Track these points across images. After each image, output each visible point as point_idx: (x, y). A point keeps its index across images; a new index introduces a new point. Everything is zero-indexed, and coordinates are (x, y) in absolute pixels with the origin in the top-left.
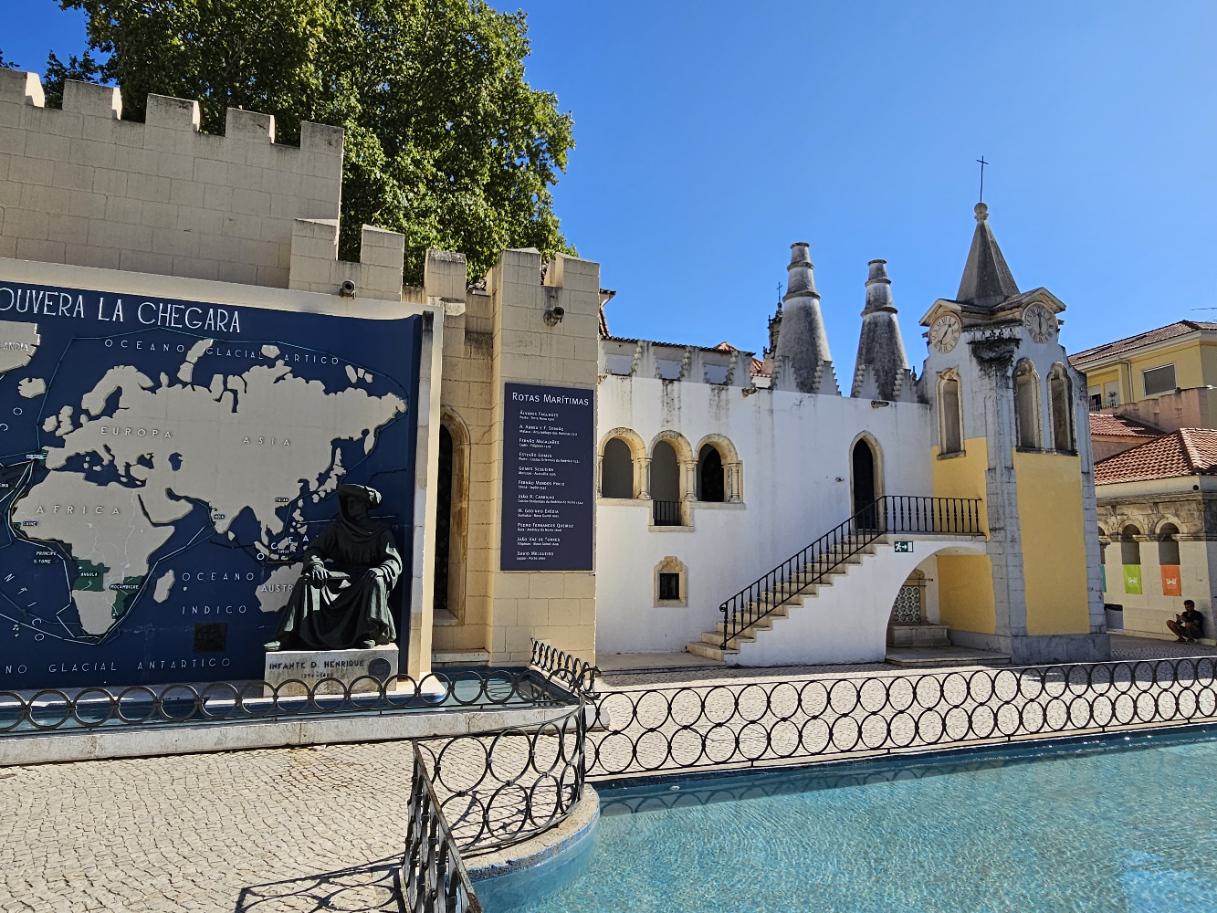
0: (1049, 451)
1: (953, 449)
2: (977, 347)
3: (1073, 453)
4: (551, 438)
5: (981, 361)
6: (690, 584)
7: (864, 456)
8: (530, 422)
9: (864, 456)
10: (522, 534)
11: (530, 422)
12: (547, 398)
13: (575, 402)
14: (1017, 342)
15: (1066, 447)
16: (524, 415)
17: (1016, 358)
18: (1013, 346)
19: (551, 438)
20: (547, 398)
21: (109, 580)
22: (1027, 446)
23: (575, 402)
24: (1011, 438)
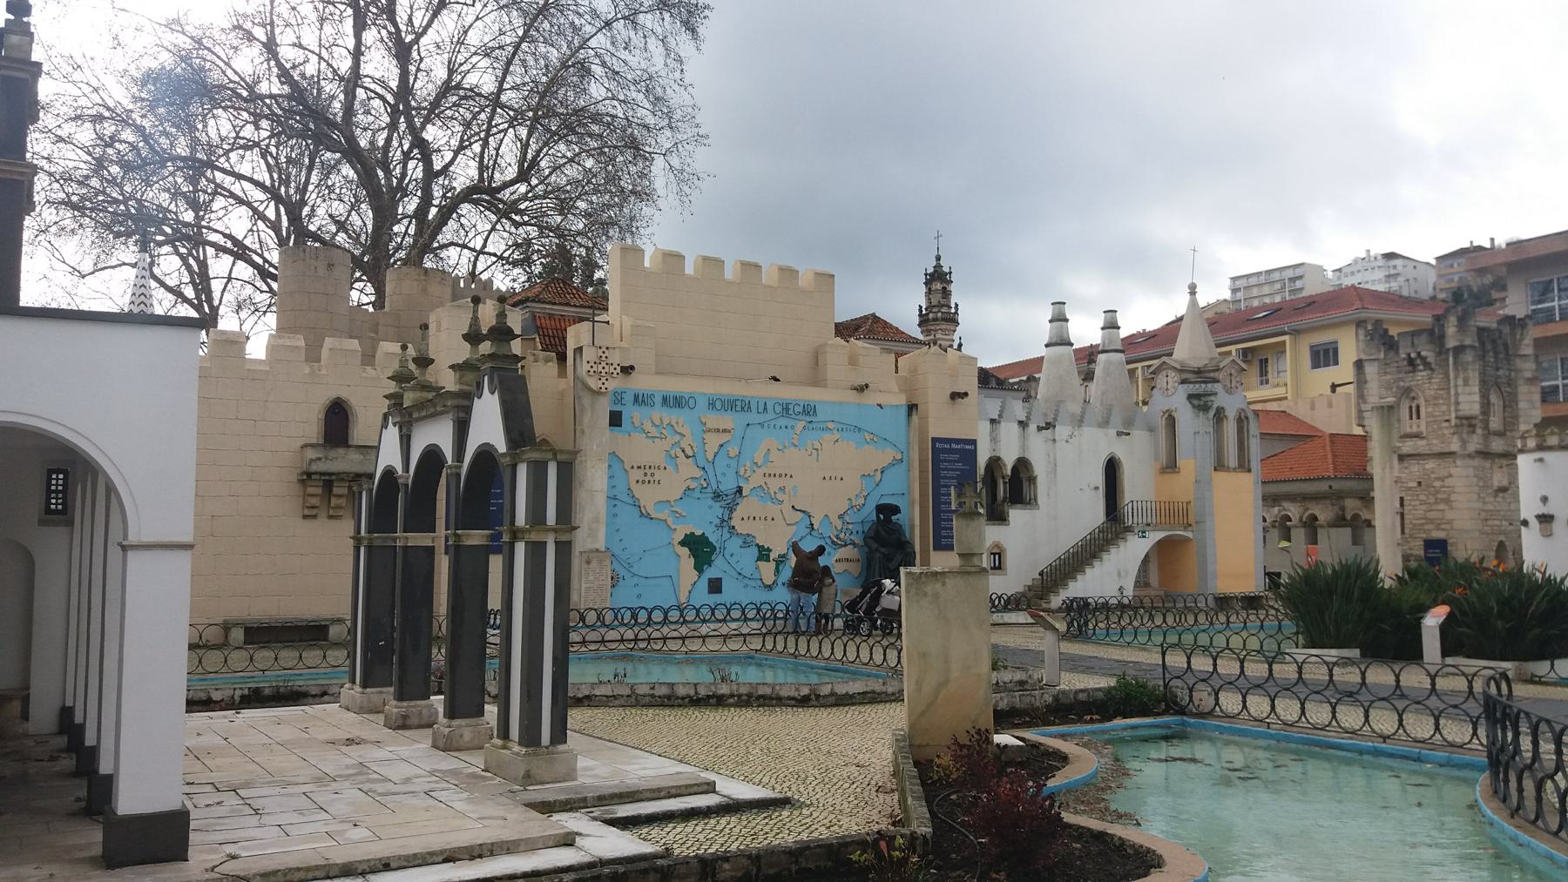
0: (1235, 469)
1: (1171, 466)
2: (1191, 397)
3: (1249, 471)
4: (957, 470)
5: (1194, 406)
6: (1010, 560)
7: (1112, 468)
8: (945, 461)
9: (1112, 468)
10: (943, 529)
11: (945, 461)
12: (953, 446)
13: (967, 447)
14: (1215, 394)
15: (1244, 466)
16: (942, 456)
17: (1215, 406)
18: (1212, 398)
19: (957, 470)
20: (953, 446)
21: (772, 556)
22: (1220, 466)
23: (967, 447)
24: (1210, 462)
